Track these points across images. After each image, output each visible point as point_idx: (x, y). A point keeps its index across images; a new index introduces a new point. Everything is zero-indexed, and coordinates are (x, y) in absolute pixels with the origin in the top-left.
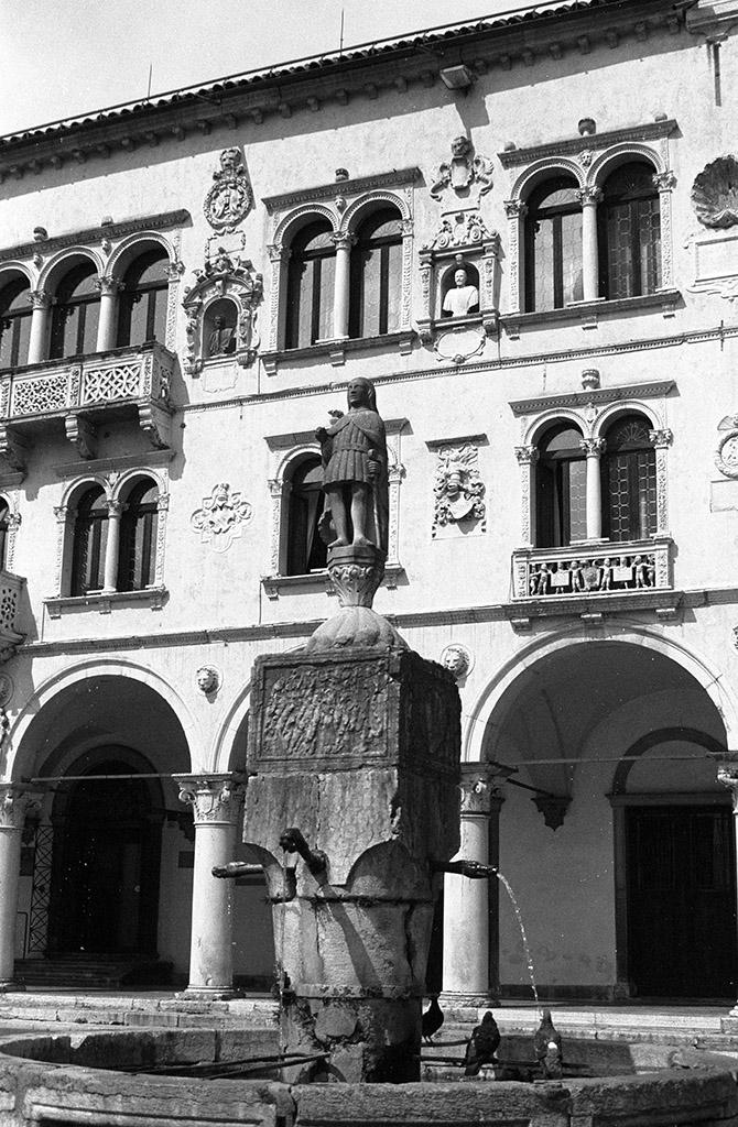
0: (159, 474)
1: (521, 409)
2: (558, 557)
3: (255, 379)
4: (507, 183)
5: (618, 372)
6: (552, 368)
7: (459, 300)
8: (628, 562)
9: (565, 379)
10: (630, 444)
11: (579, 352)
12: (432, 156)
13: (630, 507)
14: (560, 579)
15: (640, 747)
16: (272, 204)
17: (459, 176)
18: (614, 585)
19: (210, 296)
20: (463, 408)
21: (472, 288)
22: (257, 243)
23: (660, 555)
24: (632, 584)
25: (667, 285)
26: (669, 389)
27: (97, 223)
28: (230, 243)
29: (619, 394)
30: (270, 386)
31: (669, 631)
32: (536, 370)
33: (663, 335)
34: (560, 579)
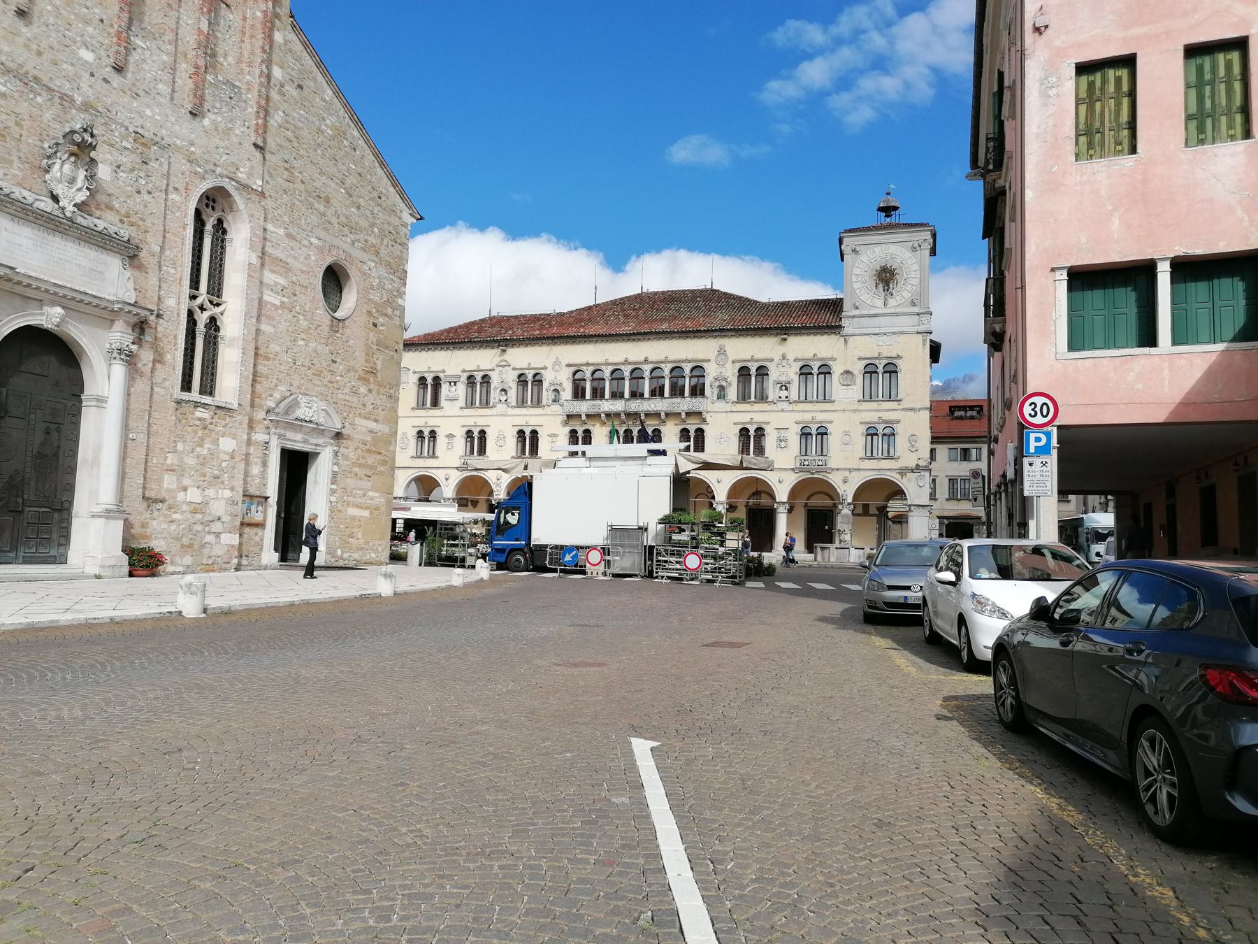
0: (704, 427)
3: (729, 407)
5: (821, 417)
7: (784, 393)
17: (784, 363)
19: (717, 384)
22: (731, 373)
26: (831, 422)
28: (723, 370)
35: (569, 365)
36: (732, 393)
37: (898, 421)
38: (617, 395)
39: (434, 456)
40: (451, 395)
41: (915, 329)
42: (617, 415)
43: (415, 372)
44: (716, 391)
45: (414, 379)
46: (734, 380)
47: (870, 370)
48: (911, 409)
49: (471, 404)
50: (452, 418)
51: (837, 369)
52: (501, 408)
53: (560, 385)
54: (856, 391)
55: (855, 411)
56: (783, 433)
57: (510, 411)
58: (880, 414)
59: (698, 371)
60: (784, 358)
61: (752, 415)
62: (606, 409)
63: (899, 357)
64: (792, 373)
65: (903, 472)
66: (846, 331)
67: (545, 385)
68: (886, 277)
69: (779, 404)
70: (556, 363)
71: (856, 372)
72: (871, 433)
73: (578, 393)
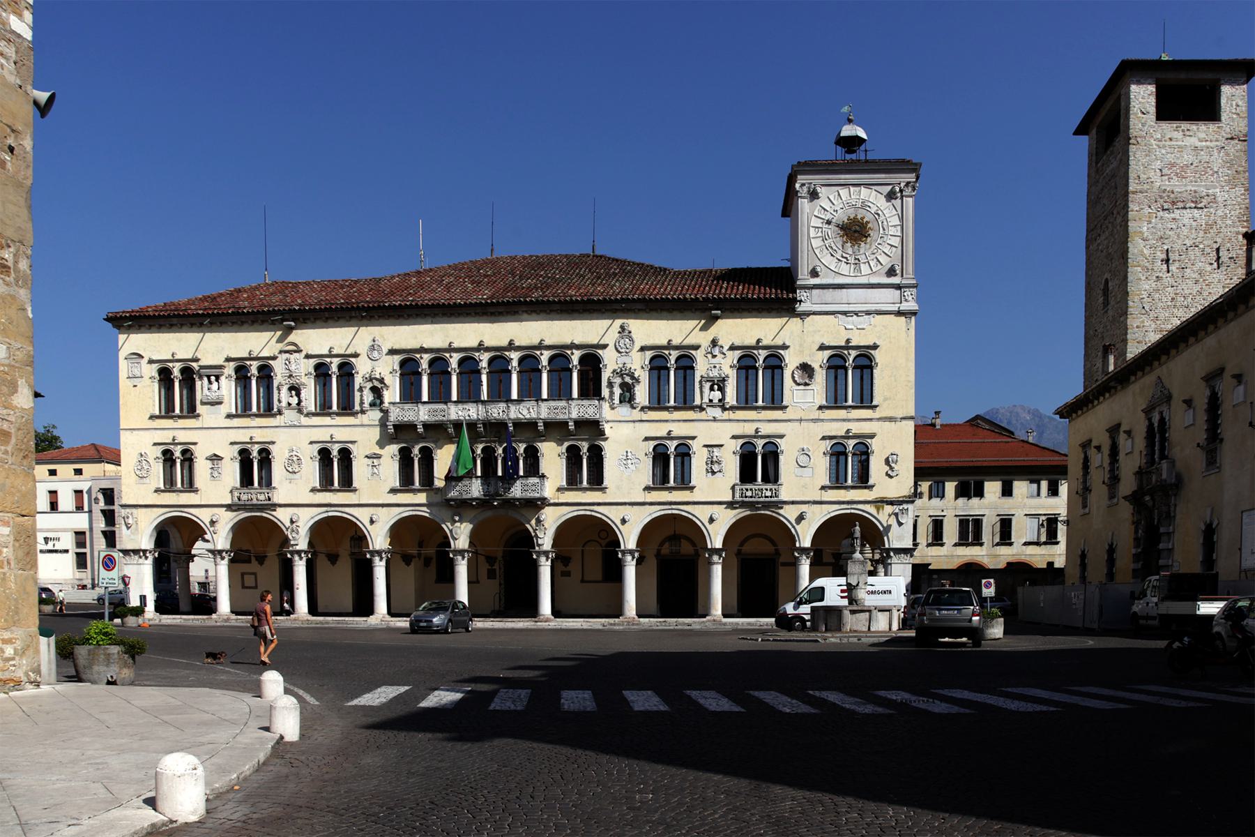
2: (749, 486)
3: (636, 414)
6: (746, 424)
7: (717, 395)
12: (704, 339)
13: (772, 476)
14: (749, 494)
15: (742, 544)
16: (643, 349)
17: (716, 351)
20: (715, 434)
22: (638, 363)
25: (785, 403)
26: (781, 437)
27: (568, 342)
29: (768, 436)
30: (645, 417)
31: (781, 511)
32: (742, 424)
34: (749, 494)
35: (392, 352)
36: (642, 394)
37: (872, 436)
38: (469, 394)
39: (190, 486)
40: (213, 396)
41: (895, 308)
42: (472, 425)
43: (151, 362)
44: (617, 391)
45: (153, 370)
46: (644, 376)
47: (836, 365)
48: (891, 419)
49: (244, 410)
50: (215, 433)
51: (791, 361)
52: (290, 416)
53: (382, 381)
54: (818, 390)
56: (716, 451)
57: (305, 421)
59: (591, 363)
60: (714, 343)
61: (676, 424)
62: (453, 417)
63: (875, 347)
64: (727, 365)
66: (801, 308)
67: (358, 380)
69: (709, 409)
70: (374, 348)
71: (816, 366)
72: (838, 454)
73: (410, 394)
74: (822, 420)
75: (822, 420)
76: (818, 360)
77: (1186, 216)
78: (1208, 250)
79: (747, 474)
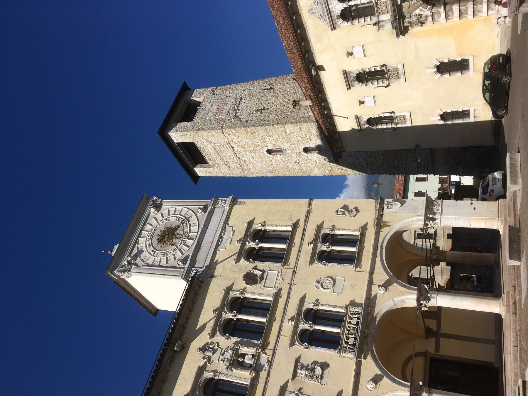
1: (292, 344)
4: (219, 338)
5: (292, 311)
6: (282, 333)
8: (347, 338)
9: (288, 326)
10: (314, 316)
11: (281, 324)
18: (357, 324)
21: (246, 357)
23: (352, 309)
24: (358, 319)
26: (302, 300)
29: (299, 313)
32: (281, 337)
33: (285, 300)
41: (227, 208)
47: (253, 255)
54: (272, 269)
55: (294, 273)
58: (305, 244)
63: (250, 224)
65: (380, 224)
68: (168, 236)
74: (296, 266)
75: (296, 266)
76: (246, 265)
77: (243, 105)
78: (263, 95)
79: (331, 342)
